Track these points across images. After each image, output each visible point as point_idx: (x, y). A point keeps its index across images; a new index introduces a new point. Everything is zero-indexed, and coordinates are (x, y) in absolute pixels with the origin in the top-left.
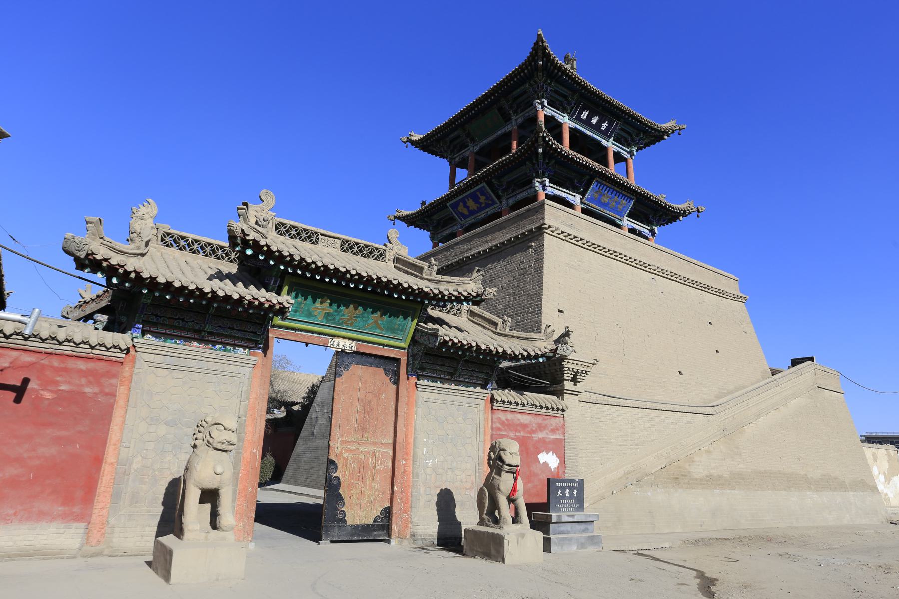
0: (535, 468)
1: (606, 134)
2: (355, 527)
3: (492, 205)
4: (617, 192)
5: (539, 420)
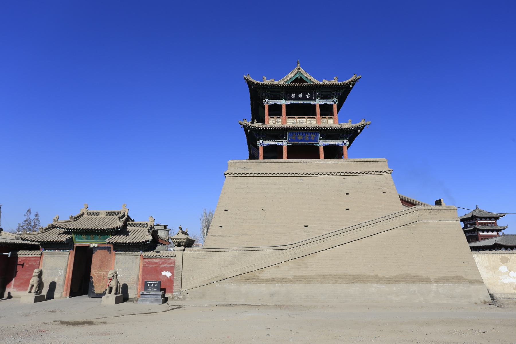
0: (160, 277)
1: (311, 99)
2: (98, 294)
5: (163, 261)
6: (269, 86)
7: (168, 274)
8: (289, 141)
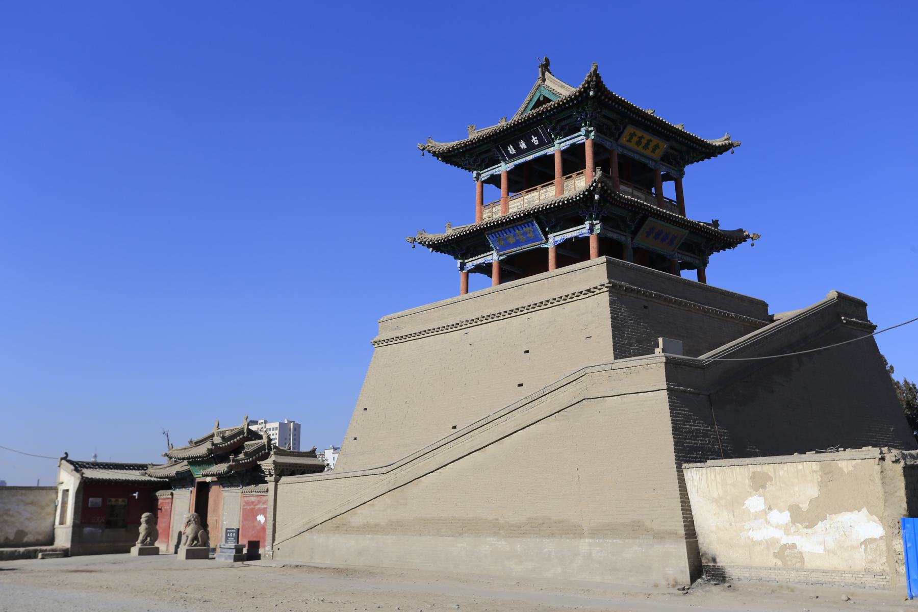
1: (542, 145)
4: (520, 225)
5: (258, 498)
6: (458, 149)
7: (261, 518)
8: (498, 251)
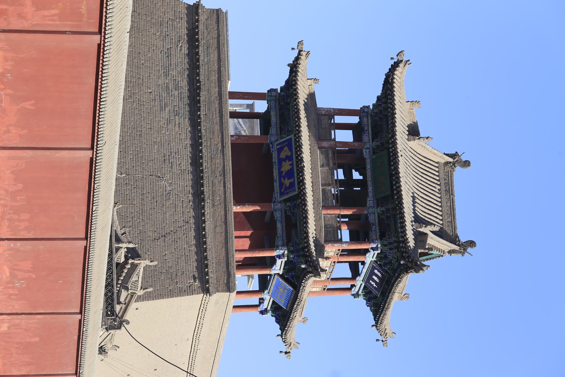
3: (281, 189)
